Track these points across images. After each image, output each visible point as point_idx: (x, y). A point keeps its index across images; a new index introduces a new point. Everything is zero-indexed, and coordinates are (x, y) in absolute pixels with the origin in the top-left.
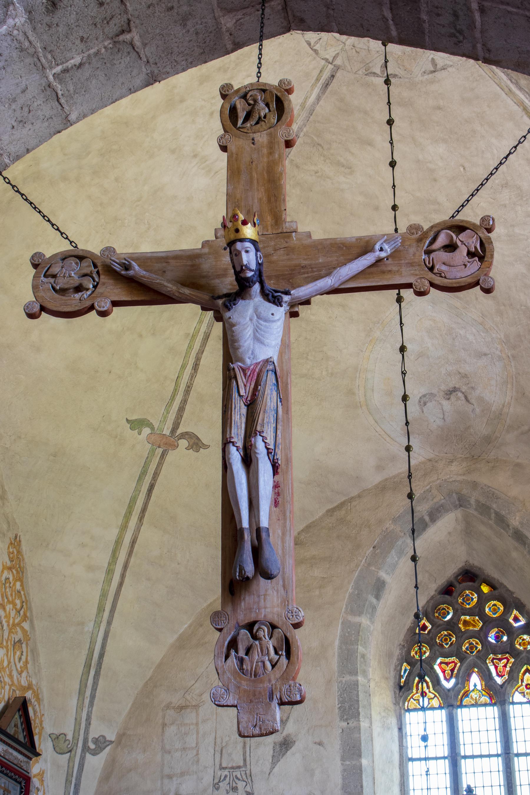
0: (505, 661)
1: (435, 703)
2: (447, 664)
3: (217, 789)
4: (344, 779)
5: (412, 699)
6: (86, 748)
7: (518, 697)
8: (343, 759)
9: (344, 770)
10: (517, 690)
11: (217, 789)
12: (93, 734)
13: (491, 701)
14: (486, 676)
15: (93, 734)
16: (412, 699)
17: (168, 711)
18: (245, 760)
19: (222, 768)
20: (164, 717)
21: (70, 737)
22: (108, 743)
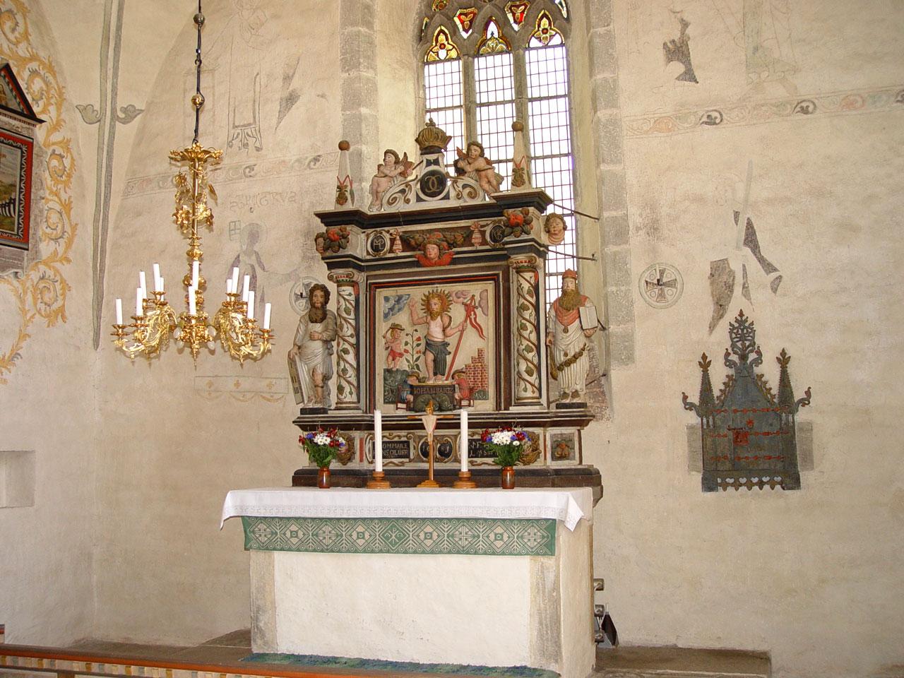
0: (523, 7)
1: (454, 54)
2: (466, 15)
3: (231, 147)
4: (344, 127)
5: (431, 53)
6: (114, 117)
7: (534, 43)
8: (344, 109)
9: (345, 120)
10: (533, 36)
11: (231, 147)
12: (122, 102)
13: (508, 48)
14: (503, 24)
15: (122, 102)
16: (431, 53)
17: (189, 77)
18: (254, 117)
19: (235, 127)
20: (185, 83)
21: (97, 107)
22: (137, 112)
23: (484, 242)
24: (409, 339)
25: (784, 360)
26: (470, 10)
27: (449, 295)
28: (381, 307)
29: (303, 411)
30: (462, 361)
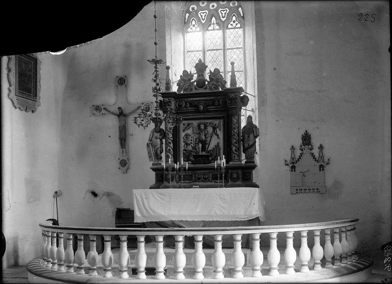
23: (219, 105)
24: (192, 139)
25: (321, 147)
26: (204, 11)
27: (207, 123)
28: (182, 127)
29: (153, 164)
30: (212, 146)
